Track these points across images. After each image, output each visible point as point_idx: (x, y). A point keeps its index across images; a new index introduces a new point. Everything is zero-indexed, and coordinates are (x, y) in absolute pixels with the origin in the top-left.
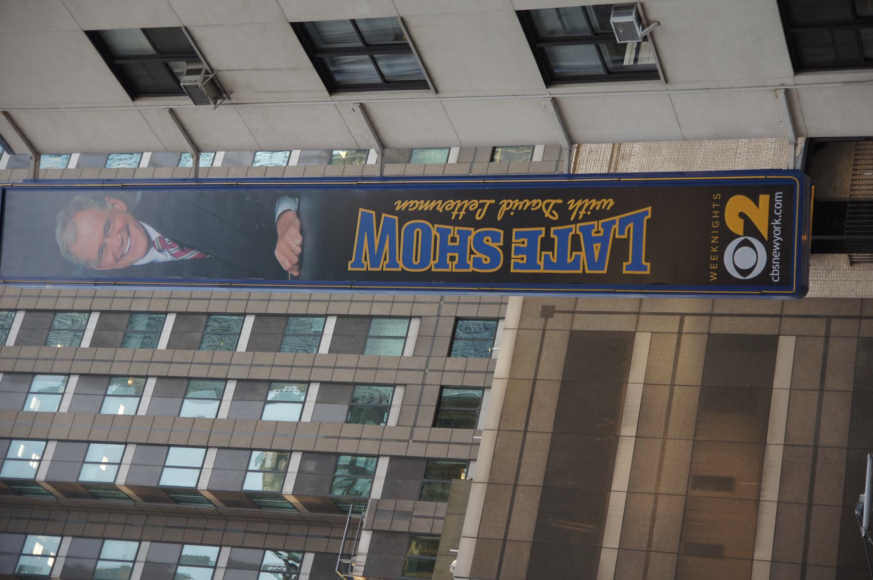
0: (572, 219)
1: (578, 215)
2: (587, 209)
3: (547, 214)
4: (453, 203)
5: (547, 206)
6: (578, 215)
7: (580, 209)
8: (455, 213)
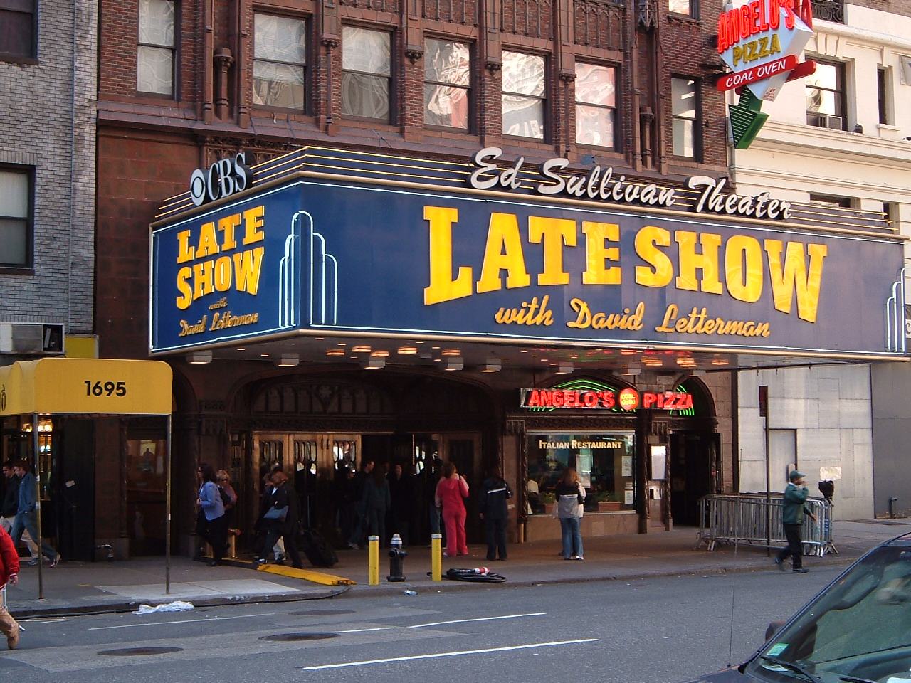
0: (546, 298)
1: (539, 303)
2: (528, 309)
3: (584, 307)
4: (706, 328)
5: (584, 320)
6: (539, 303)
7: (537, 311)
8: (703, 316)
